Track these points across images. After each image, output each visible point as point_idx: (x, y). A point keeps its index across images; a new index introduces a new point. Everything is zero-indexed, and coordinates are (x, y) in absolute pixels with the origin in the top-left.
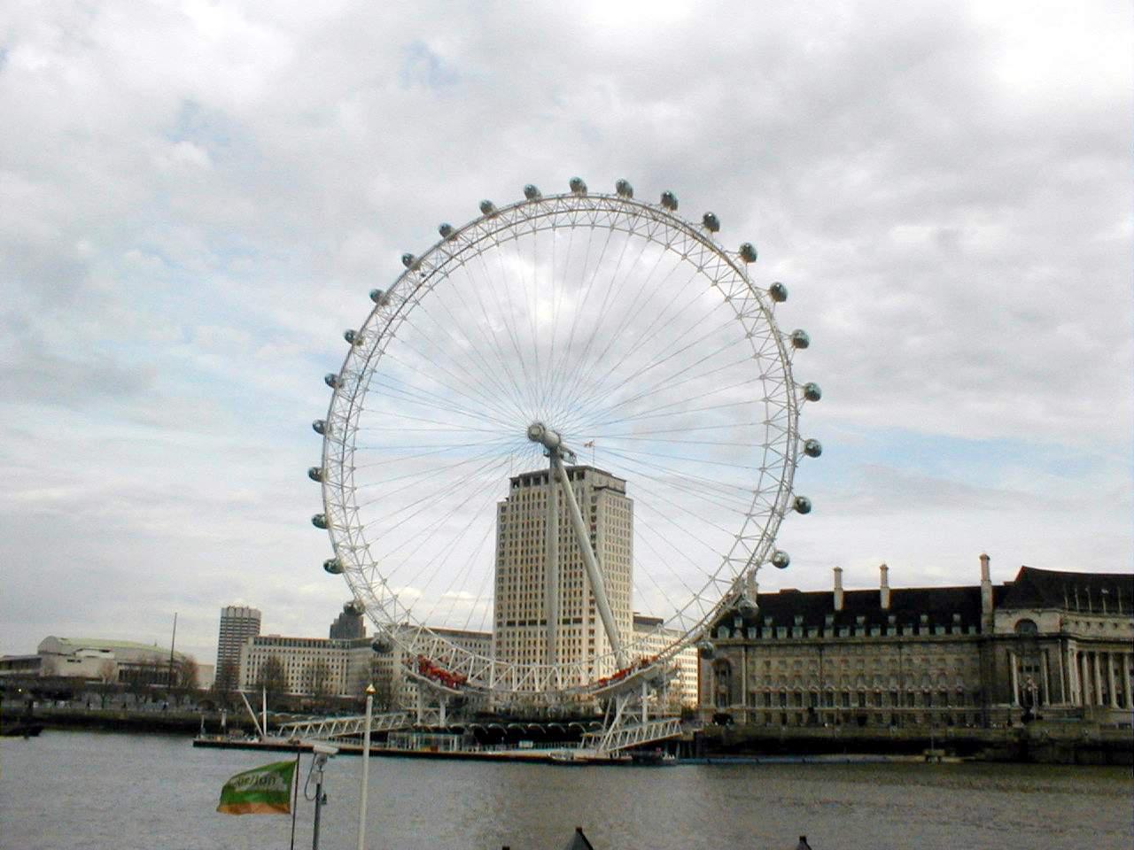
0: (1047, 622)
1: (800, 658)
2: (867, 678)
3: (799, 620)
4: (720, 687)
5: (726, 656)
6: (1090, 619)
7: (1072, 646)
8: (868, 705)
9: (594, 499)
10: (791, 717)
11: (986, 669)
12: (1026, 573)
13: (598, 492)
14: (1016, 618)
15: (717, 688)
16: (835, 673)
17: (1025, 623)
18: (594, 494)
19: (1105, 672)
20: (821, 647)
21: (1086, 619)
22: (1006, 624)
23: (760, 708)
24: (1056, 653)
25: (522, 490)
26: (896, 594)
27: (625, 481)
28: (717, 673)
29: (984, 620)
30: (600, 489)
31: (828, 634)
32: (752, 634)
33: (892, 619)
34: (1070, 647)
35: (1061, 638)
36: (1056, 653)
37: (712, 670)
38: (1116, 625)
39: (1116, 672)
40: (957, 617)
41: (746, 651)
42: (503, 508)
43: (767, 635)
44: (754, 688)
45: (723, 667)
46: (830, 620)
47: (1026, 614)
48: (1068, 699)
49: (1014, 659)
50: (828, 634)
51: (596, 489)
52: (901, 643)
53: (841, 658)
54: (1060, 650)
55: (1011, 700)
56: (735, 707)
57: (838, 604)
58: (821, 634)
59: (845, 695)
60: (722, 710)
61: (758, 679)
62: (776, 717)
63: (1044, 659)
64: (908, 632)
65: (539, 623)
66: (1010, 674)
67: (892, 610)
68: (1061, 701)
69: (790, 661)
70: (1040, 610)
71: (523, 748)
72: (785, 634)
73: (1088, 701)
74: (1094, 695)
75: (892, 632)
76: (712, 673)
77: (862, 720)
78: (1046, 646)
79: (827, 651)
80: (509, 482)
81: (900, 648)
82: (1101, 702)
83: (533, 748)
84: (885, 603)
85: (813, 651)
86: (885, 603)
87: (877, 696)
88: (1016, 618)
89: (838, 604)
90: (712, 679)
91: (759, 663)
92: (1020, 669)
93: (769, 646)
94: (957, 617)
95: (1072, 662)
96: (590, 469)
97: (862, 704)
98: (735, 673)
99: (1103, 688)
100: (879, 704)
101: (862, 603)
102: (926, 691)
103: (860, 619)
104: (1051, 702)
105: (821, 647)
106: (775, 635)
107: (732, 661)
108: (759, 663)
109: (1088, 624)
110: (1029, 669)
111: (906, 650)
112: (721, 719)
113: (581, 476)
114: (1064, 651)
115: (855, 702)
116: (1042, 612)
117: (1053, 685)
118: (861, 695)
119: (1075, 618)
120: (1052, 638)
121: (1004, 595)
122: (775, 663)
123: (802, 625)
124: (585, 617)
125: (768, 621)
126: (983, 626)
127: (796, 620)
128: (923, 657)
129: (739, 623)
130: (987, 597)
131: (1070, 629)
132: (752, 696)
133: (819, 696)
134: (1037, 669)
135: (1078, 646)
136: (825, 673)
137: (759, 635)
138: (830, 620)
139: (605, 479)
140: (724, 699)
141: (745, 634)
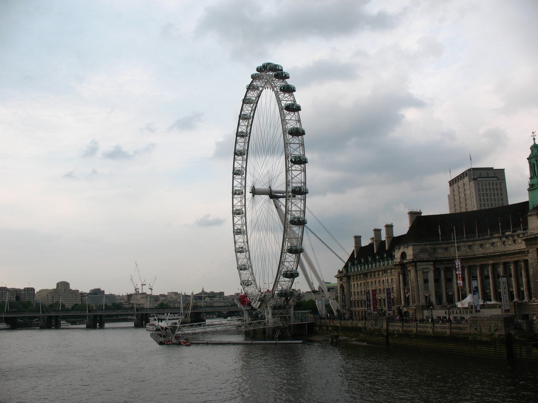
14: (401, 251)
17: (403, 255)
27: (504, 170)
34: (418, 268)
38: (470, 247)
52: (384, 269)
80: (448, 184)
88: (401, 251)
113: (466, 174)
136: (368, 289)
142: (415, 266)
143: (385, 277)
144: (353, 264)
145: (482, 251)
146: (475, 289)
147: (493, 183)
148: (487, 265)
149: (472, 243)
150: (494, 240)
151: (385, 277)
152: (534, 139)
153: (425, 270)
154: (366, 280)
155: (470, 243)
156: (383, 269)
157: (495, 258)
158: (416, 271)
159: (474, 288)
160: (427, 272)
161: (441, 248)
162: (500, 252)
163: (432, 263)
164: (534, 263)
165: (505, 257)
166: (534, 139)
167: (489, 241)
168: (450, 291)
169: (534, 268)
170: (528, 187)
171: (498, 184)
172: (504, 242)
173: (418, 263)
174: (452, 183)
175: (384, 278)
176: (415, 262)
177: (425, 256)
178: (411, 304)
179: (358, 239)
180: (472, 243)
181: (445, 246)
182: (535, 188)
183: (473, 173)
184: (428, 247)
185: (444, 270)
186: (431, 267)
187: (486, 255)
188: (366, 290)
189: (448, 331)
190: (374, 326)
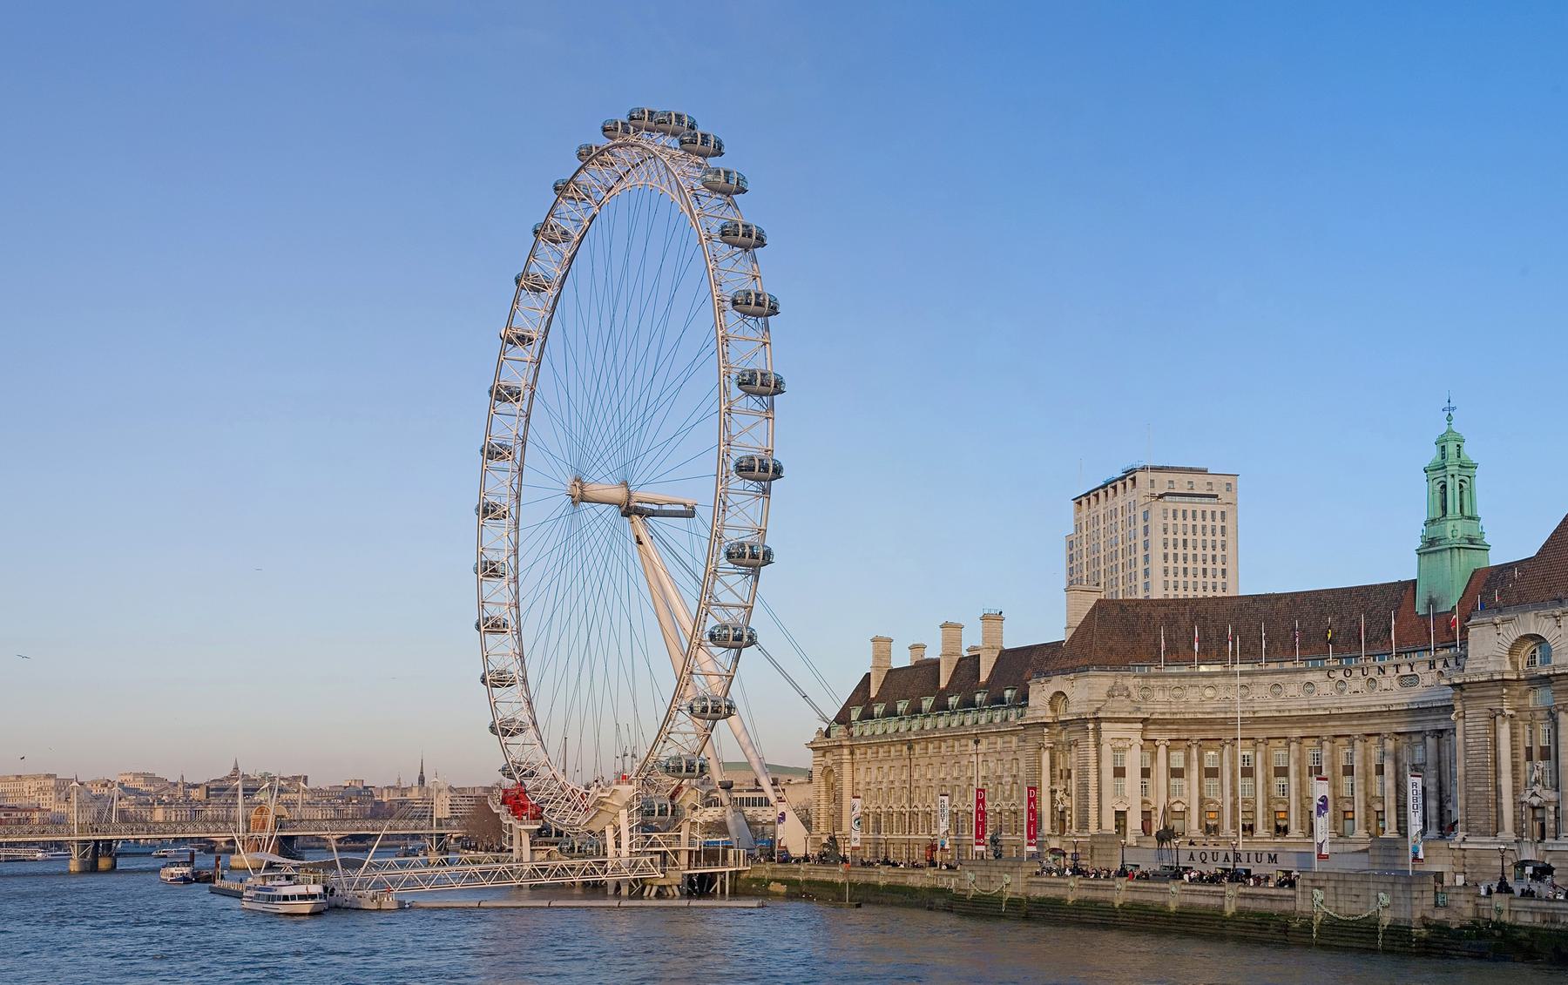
3: (902, 706)
7: (1109, 731)
9: (1146, 513)
20: (910, 745)
30: (1161, 496)
33: (978, 697)
35: (1090, 723)
48: (1100, 826)
52: (976, 734)
54: (1091, 739)
67: (987, 685)
68: (1087, 827)
91: (862, 770)
96: (1143, 469)
105: (910, 745)
113: (1134, 480)
114: (1098, 745)
120: (1082, 721)
129: (855, 715)
138: (927, 703)
142: (1098, 731)
143: (977, 754)
145: (1275, 704)
146: (1321, 803)
147: (1204, 512)
149: (1250, 681)
150: (1310, 677)
151: (977, 754)
153: (1120, 744)
156: (974, 732)
157: (1310, 725)
159: (1320, 800)
160: (1124, 750)
161: (1163, 688)
162: (1325, 709)
163: (1140, 726)
164: (1476, 744)
165: (1338, 723)
167: (1298, 678)
168: (1178, 802)
169: (1473, 756)
171: (1218, 516)
173: (1103, 725)
175: (975, 756)
176: (1098, 720)
177: (1122, 708)
178: (1074, 829)
179: (882, 645)
180: (1250, 681)
181: (1174, 682)
182: (1437, 548)
183: (1152, 481)
184: (1131, 682)
185: (1167, 747)
186: (1137, 738)
187: (1287, 714)
189: (1230, 906)
190: (978, 883)
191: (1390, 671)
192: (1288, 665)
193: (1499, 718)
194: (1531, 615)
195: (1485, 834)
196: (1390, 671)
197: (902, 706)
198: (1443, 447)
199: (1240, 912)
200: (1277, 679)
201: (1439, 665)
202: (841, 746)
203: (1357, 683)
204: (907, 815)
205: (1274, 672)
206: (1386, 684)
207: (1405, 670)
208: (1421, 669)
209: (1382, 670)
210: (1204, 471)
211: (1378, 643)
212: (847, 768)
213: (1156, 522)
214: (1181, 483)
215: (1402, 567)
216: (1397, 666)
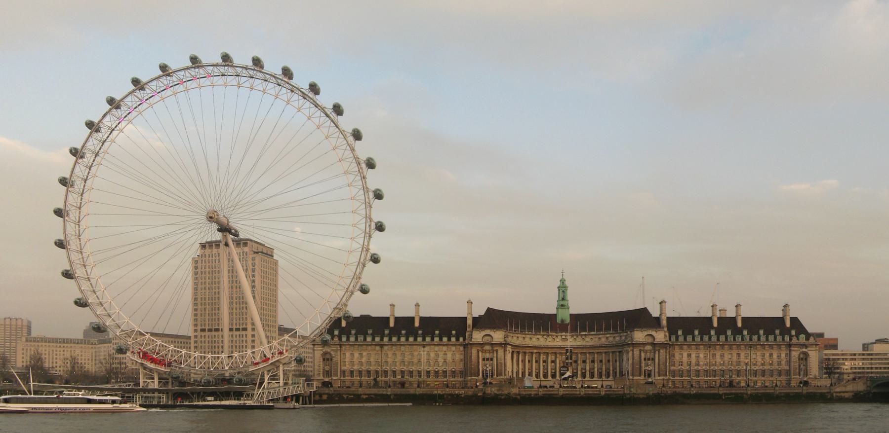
0: (498, 336)
1: (370, 352)
2: (406, 363)
4: (326, 367)
5: (329, 350)
6: (519, 335)
7: (509, 348)
8: (407, 377)
9: (253, 259)
10: (364, 384)
11: (467, 359)
12: (489, 310)
13: (256, 255)
15: (324, 368)
16: (389, 360)
18: (254, 255)
19: (524, 361)
20: (382, 346)
21: (517, 335)
22: (478, 336)
23: (348, 378)
24: (501, 352)
25: (208, 251)
26: (422, 319)
28: (324, 360)
29: (467, 334)
31: (386, 339)
32: (344, 339)
35: (504, 345)
36: (501, 352)
37: (321, 358)
39: (529, 361)
40: (454, 332)
41: (341, 347)
42: (196, 262)
43: (352, 339)
44: (344, 368)
45: (328, 356)
46: (387, 332)
47: (488, 332)
48: (505, 375)
49: (480, 354)
50: (386, 339)
51: (255, 253)
52: (424, 345)
53: (392, 352)
55: (479, 375)
56: (334, 378)
57: (392, 324)
58: (382, 339)
59: (394, 372)
60: (327, 380)
61: (347, 363)
62: (356, 384)
63: (495, 355)
64: (428, 339)
65: (234, 330)
66: (478, 362)
67: (420, 328)
69: (365, 354)
70: (495, 330)
71: (208, 401)
72: (362, 338)
73: (515, 376)
74: (517, 373)
75: (420, 339)
76: (322, 360)
77: (403, 384)
78: (495, 349)
79: (386, 348)
81: (424, 347)
82: (520, 376)
83: (214, 401)
84: (417, 324)
85: (378, 348)
86: (417, 324)
87: (411, 373)
88: (483, 333)
89: (392, 324)
90: (321, 363)
92: (483, 359)
93: (353, 345)
94: (454, 332)
95: (509, 356)
96: (251, 240)
97: (402, 377)
98: (334, 359)
99: (522, 369)
100: (412, 376)
101: (405, 326)
102: (437, 370)
103: (403, 332)
104: (497, 376)
105: (382, 346)
106: (356, 339)
107: (332, 353)
108: (348, 355)
109: (518, 337)
110: (488, 359)
111: (427, 348)
112: (326, 384)
114: (505, 351)
115: (399, 376)
116: (496, 331)
117: (499, 368)
118: (403, 372)
119: (512, 335)
120: (500, 345)
121: (479, 323)
122: (356, 355)
123: (372, 334)
124: (249, 327)
125: (353, 332)
126: (467, 338)
127: (369, 332)
128: (436, 352)
130: (469, 322)
131: (509, 340)
132: (343, 373)
133: (380, 373)
134: (492, 359)
135: (512, 348)
136: (383, 360)
137: (348, 339)
138: (387, 332)
139: (261, 247)
140: (328, 373)
141: (340, 339)
144: (345, 332)
148: (532, 353)
150: (538, 336)
152: (563, 275)
154: (382, 351)
155: (524, 336)
158: (505, 351)
166: (563, 275)
167: (535, 336)
170: (556, 306)
172: (546, 339)
173: (508, 346)
174: (203, 246)
188: (380, 361)
191: (559, 337)
192: (530, 333)
193: (642, 352)
194: (651, 331)
195: (638, 376)
196: (559, 337)
197: (370, 331)
198: (563, 282)
199: (605, 394)
200: (531, 336)
201: (575, 337)
202: (338, 344)
203: (550, 339)
204: (380, 371)
205: (530, 334)
206: (558, 340)
207: (564, 337)
208: (569, 337)
209: (557, 336)
210: (263, 245)
211: (554, 329)
212: (339, 352)
213: (257, 261)
214: (260, 248)
215: (553, 311)
216: (561, 336)
